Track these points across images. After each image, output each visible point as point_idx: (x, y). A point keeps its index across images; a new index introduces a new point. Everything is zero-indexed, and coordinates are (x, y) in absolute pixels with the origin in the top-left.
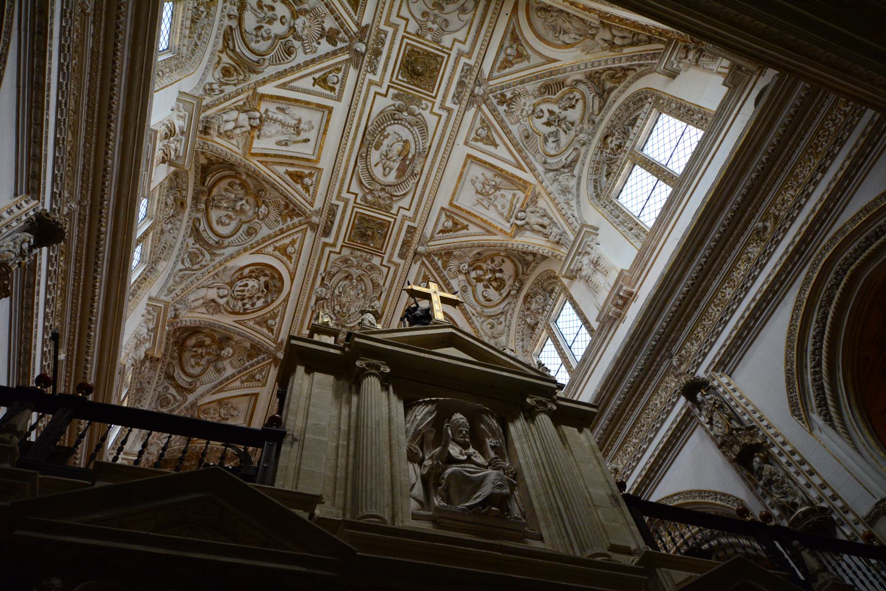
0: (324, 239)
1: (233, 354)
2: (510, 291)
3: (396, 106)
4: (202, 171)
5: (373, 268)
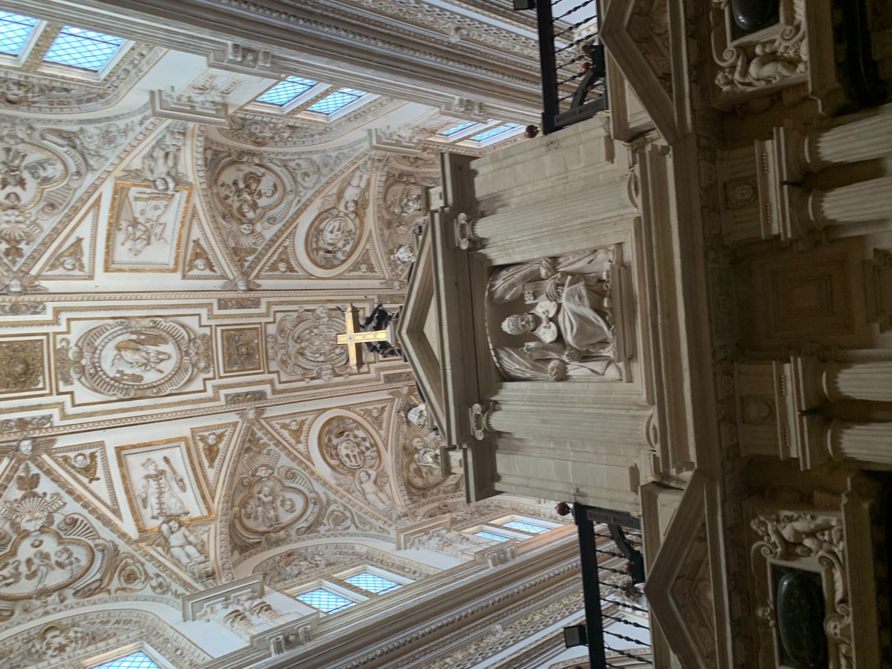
1: (418, 437)
3: (78, 376)
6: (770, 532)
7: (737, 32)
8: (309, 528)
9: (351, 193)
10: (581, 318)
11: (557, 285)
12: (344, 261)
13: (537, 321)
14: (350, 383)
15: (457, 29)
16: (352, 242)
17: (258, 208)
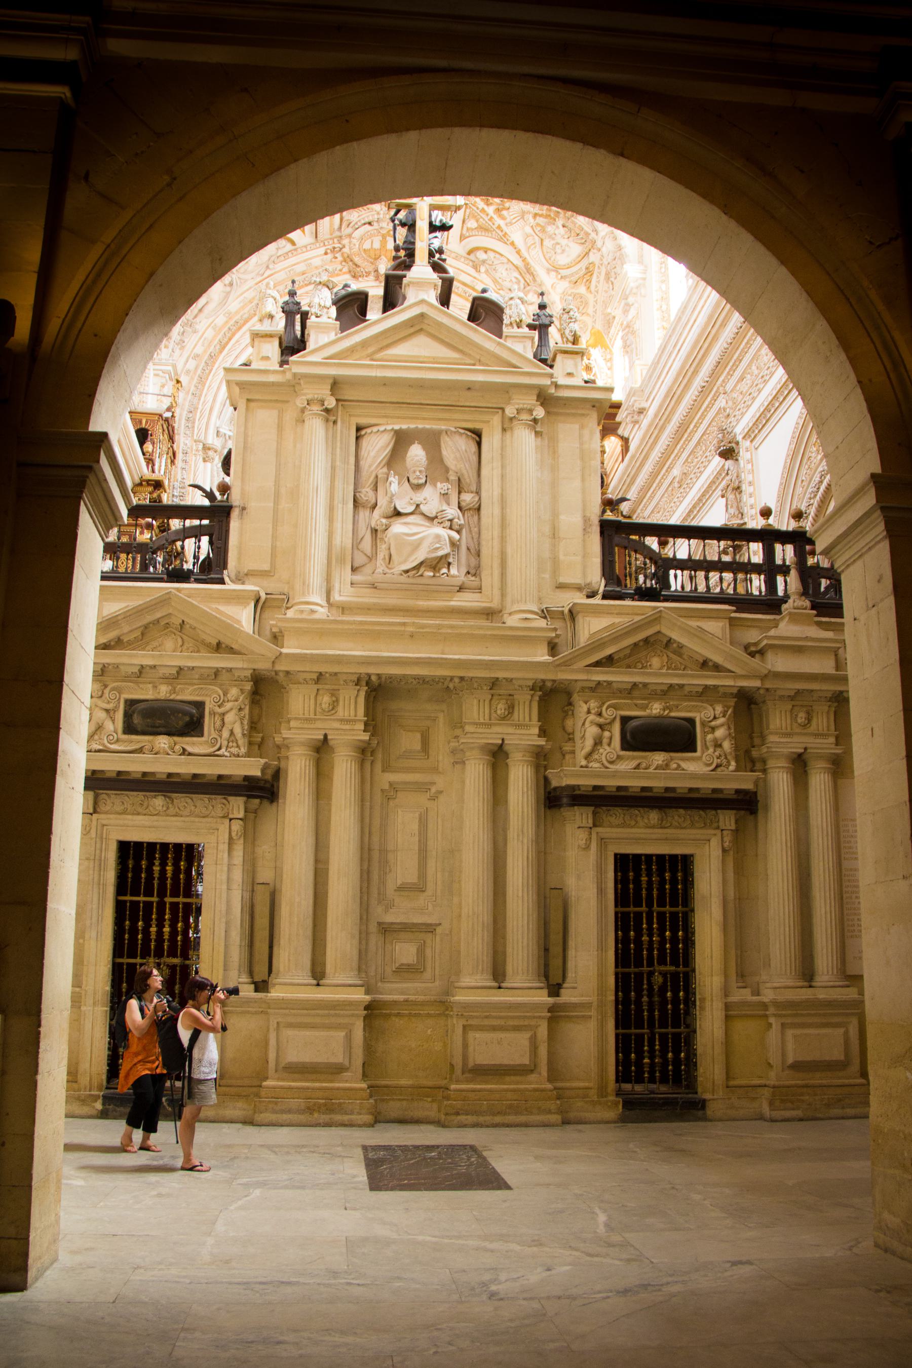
7: (625, 720)
10: (417, 546)
11: (451, 520)
13: (417, 487)
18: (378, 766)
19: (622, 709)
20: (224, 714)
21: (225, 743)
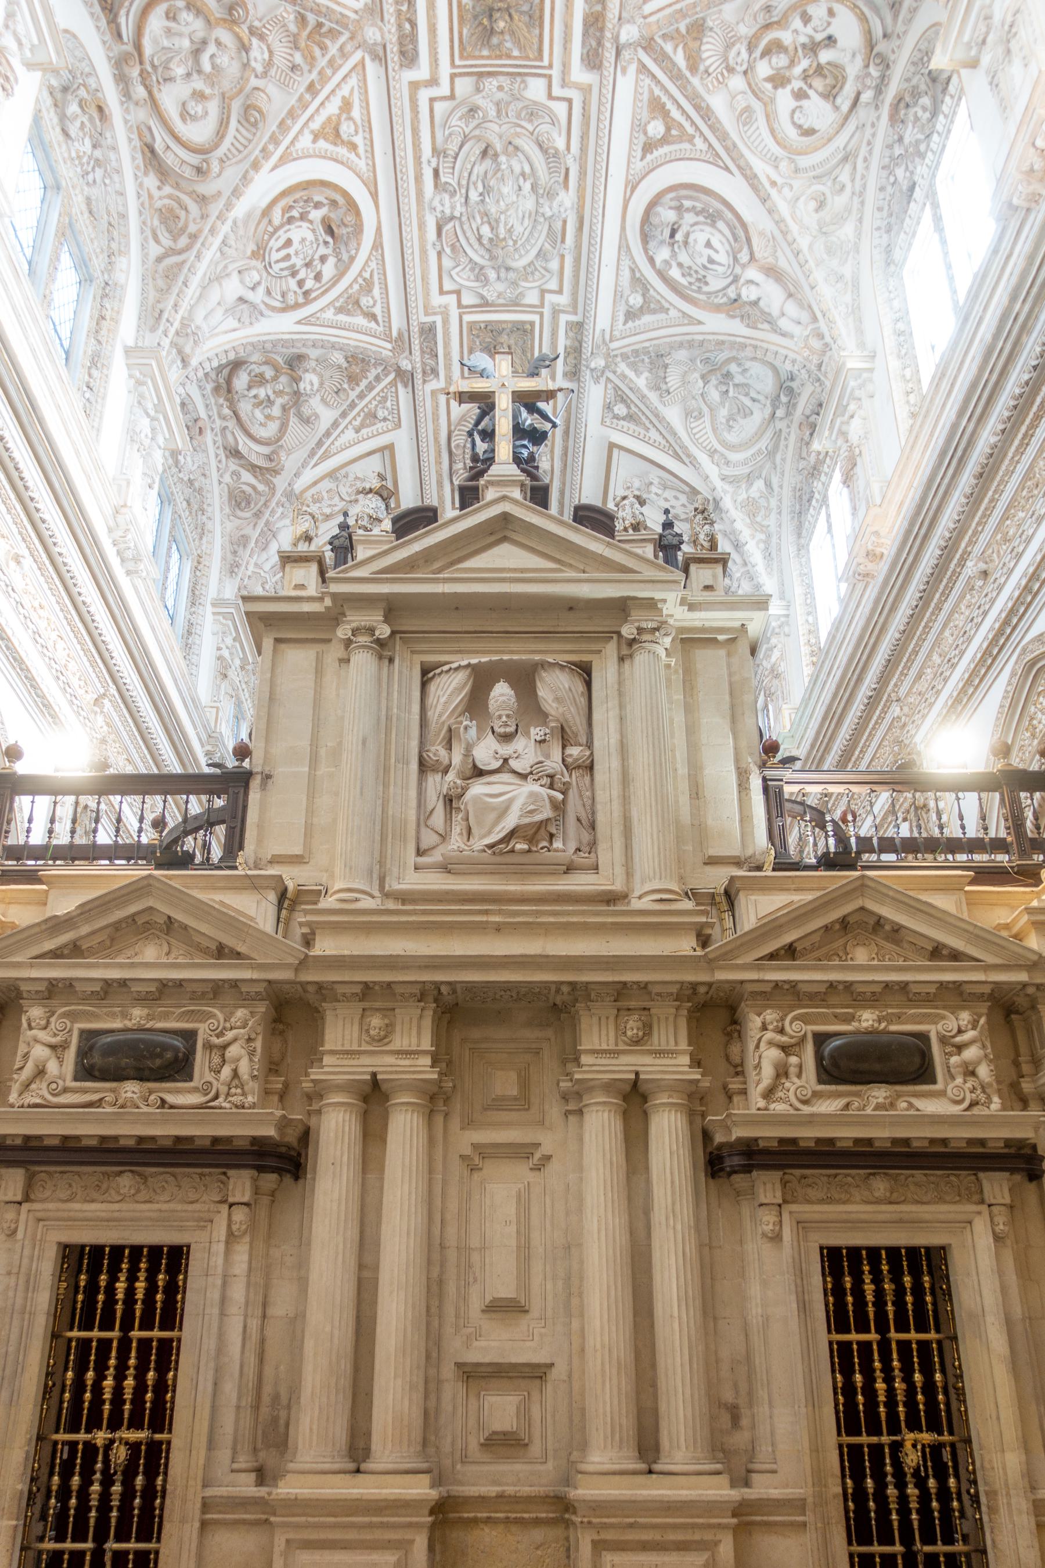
0: (410, 75)
2: (858, 95)
4: (104, 9)
5: (533, 112)
6: (235, 1031)
7: (820, 1039)
8: (152, 151)
9: (772, 295)
11: (551, 777)
12: (651, 261)
13: (507, 738)
14: (424, 252)
15: (985, 574)
16: (684, 281)
17: (775, 88)
18: (455, 1123)
19: (815, 1023)
20: (225, 1047)
21: (223, 1089)
